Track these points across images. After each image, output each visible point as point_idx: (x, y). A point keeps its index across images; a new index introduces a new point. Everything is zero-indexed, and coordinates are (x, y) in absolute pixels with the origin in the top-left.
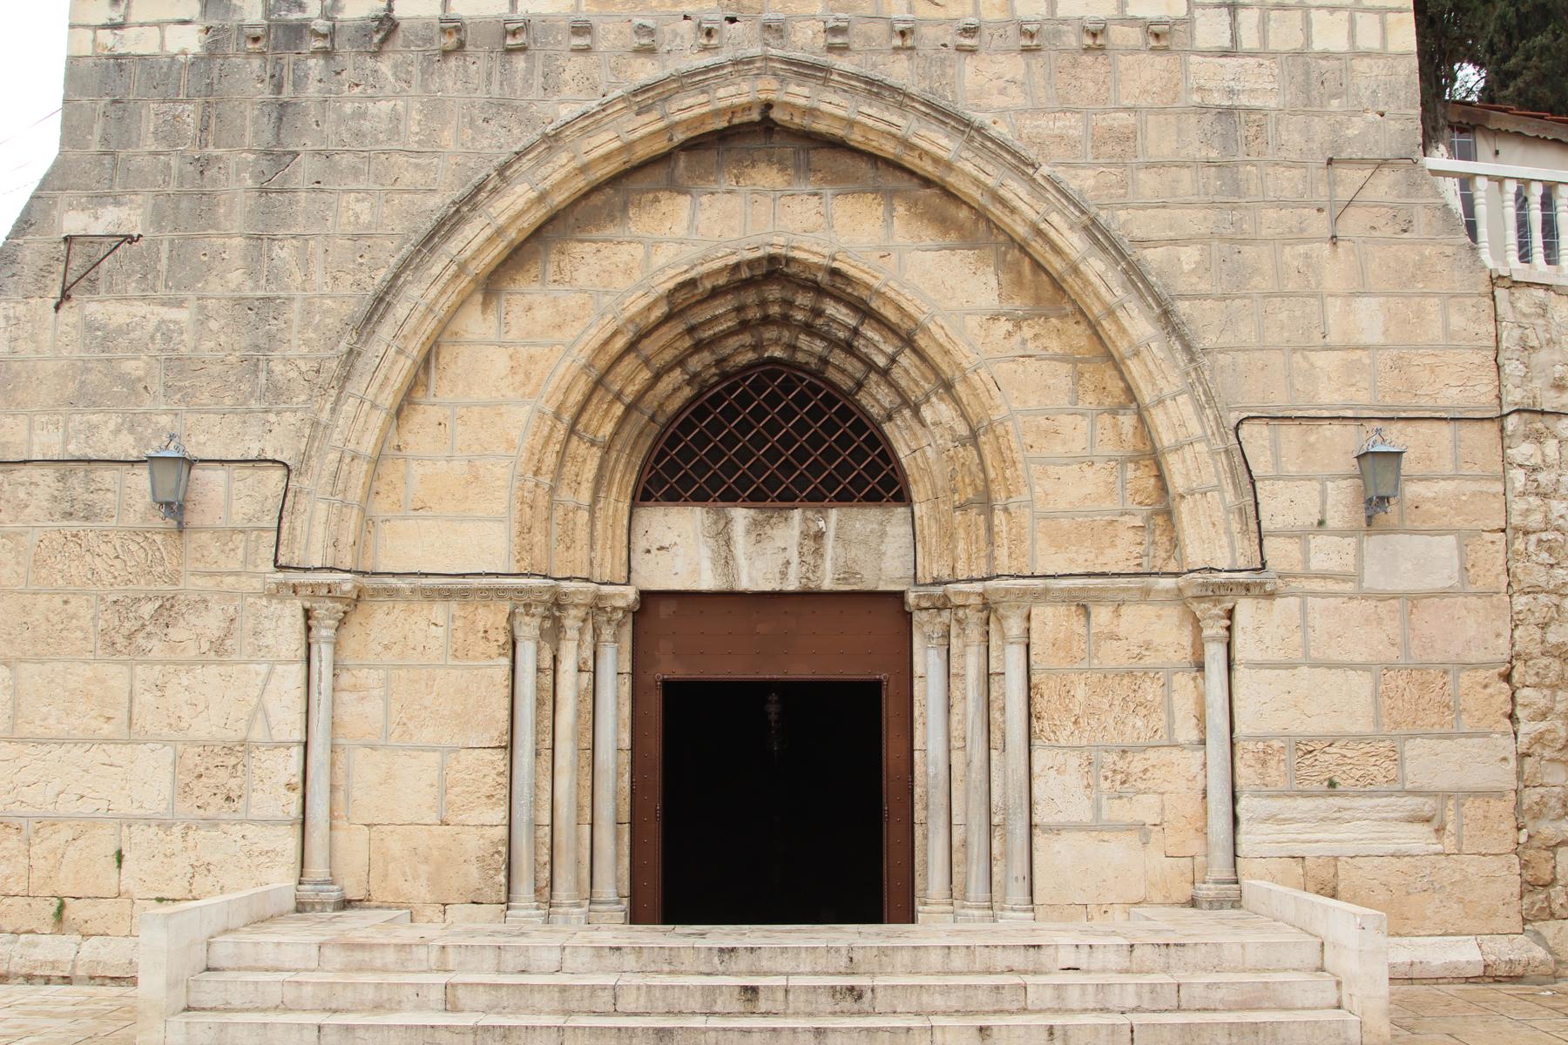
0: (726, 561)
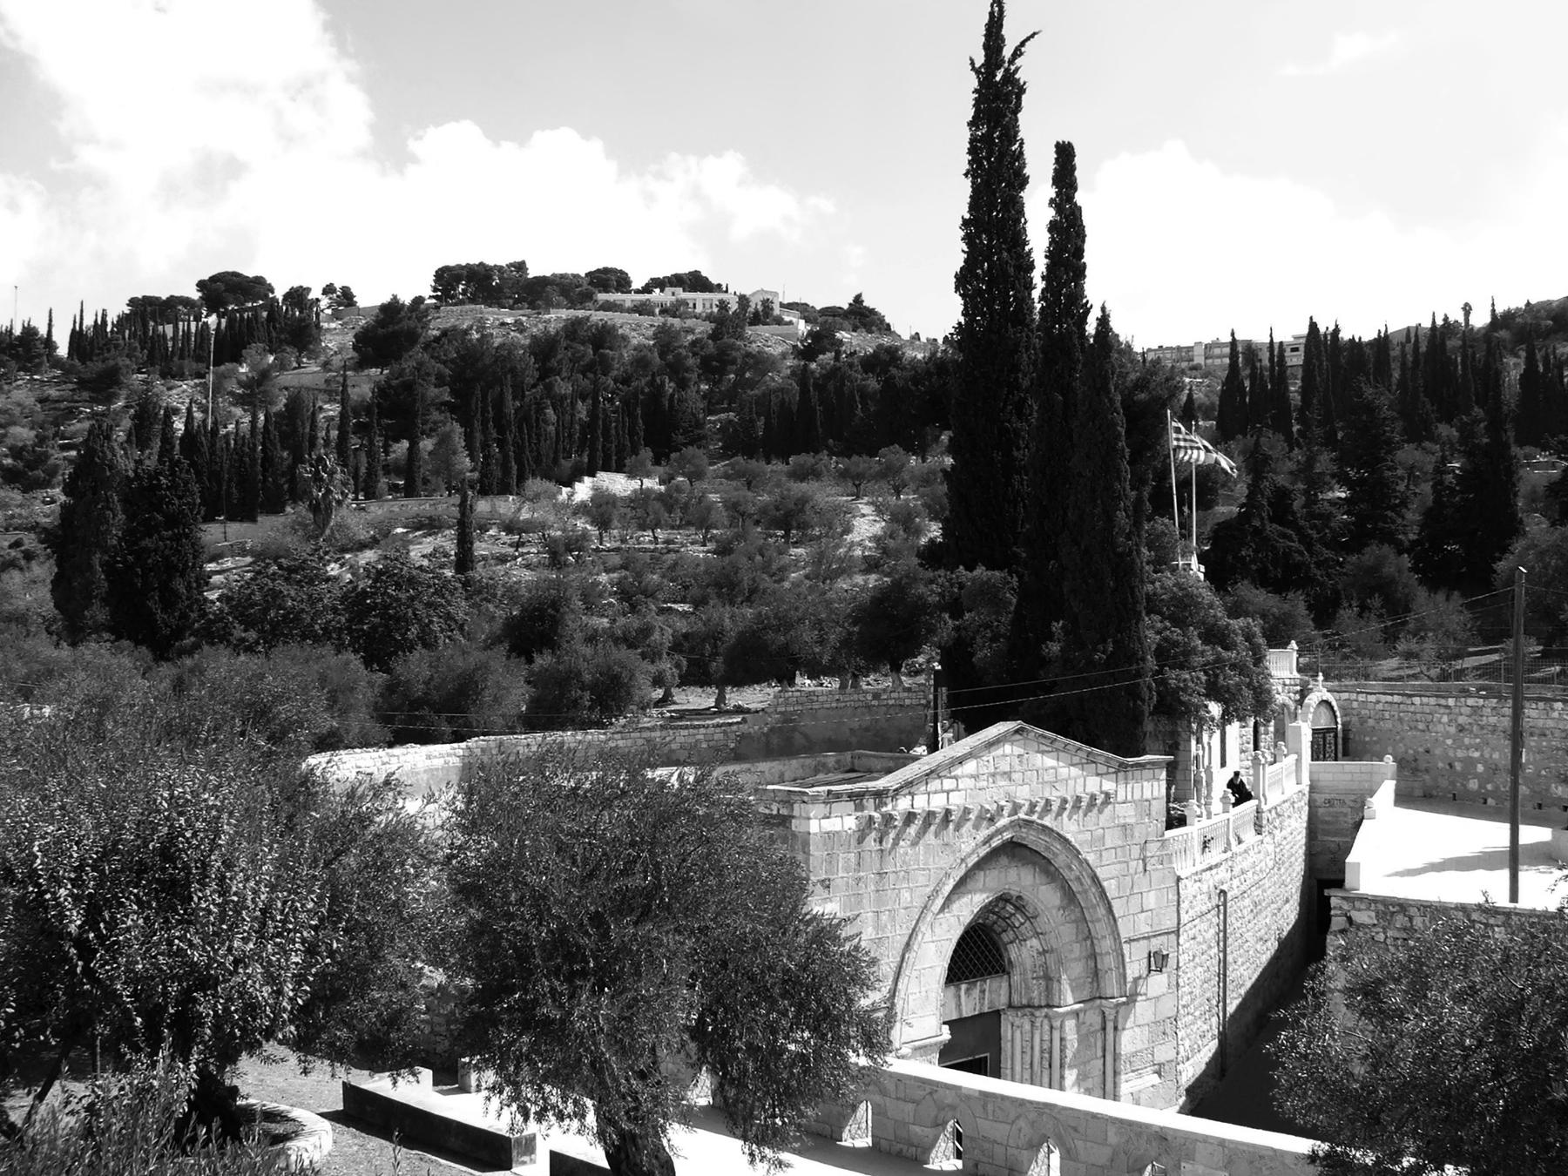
0: (959, 1005)
